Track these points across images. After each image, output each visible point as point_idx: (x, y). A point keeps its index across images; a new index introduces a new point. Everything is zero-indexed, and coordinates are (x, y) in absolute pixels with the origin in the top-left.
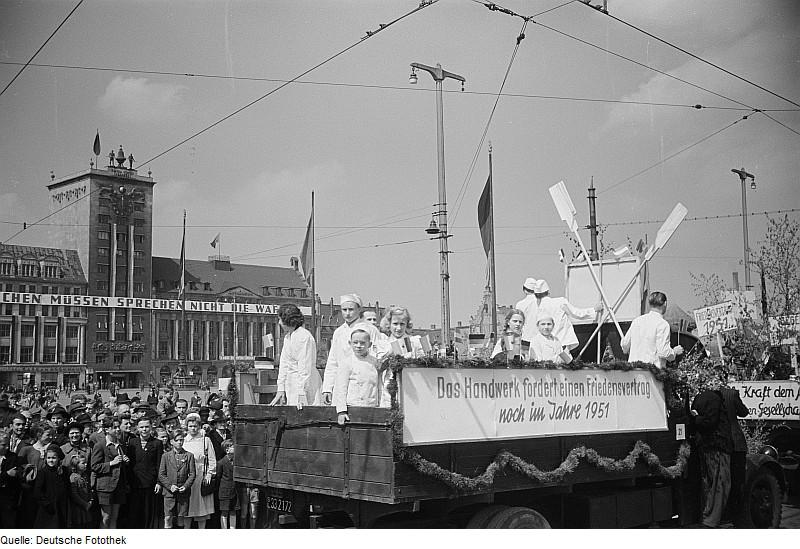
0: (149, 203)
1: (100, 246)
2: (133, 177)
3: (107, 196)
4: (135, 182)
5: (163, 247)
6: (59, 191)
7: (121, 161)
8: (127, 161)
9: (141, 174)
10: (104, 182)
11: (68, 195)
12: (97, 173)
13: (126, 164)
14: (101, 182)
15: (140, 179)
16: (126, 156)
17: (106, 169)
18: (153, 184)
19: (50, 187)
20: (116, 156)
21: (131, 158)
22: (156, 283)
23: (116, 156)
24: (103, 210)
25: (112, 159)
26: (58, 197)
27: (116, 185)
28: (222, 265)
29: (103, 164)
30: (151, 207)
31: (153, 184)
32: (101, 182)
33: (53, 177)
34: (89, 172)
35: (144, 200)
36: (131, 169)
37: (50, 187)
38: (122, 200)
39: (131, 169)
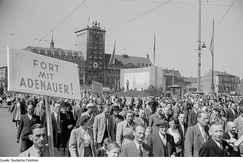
1: (91, 52)
4: (100, 31)
5: (108, 51)
7: (96, 24)
8: (98, 24)
9: (102, 28)
10: (91, 31)
12: (90, 28)
14: (90, 31)
15: (101, 30)
16: (98, 23)
18: (105, 31)
20: (95, 23)
21: (99, 24)
22: (106, 62)
23: (95, 23)
26: (78, 35)
27: (95, 32)
28: (126, 56)
31: (105, 31)
32: (90, 31)
34: (87, 28)
36: (99, 27)
37: (75, 33)
38: (96, 36)
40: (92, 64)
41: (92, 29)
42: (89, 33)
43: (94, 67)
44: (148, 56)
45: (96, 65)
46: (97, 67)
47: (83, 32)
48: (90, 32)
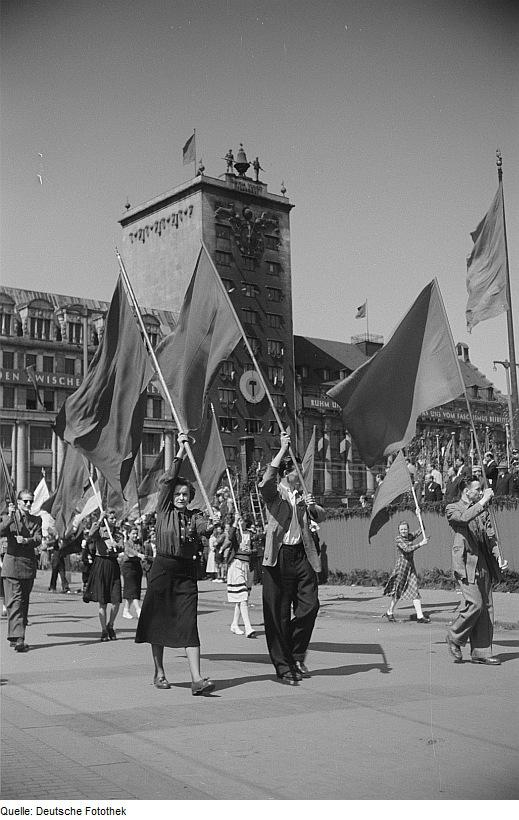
0: (285, 239)
2: (262, 194)
3: (226, 222)
6: (140, 224)
7: (242, 167)
8: (252, 167)
9: (272, 190)
10: (222, 199)
11: (158, 228)
13: (250, 173)
14: (217, 199)
15: (269, 197)
16: (250, 159)
17: (224, 178)
18: (287, 208)
19: (125, 222)
20: (236, 160)
21: (257, 167)
24: (222, 244)
25: (230, 164)
27: (239, 205)
29: (218, 172)
30: (289, 242)
31: (287, 208)
32: (217, 199)
33: (128, 207)
35: (278, 232)
37: (125, 222)
38: (248, 230)
39: (257, 182)
40: (235, 382)
41: (227, 185)
42: (209, 209)
43: (249, 398)
44: (466, 350)
45: (253, 383)
46: (258, 399)
47: (174, 208)
48: (216, 205)
